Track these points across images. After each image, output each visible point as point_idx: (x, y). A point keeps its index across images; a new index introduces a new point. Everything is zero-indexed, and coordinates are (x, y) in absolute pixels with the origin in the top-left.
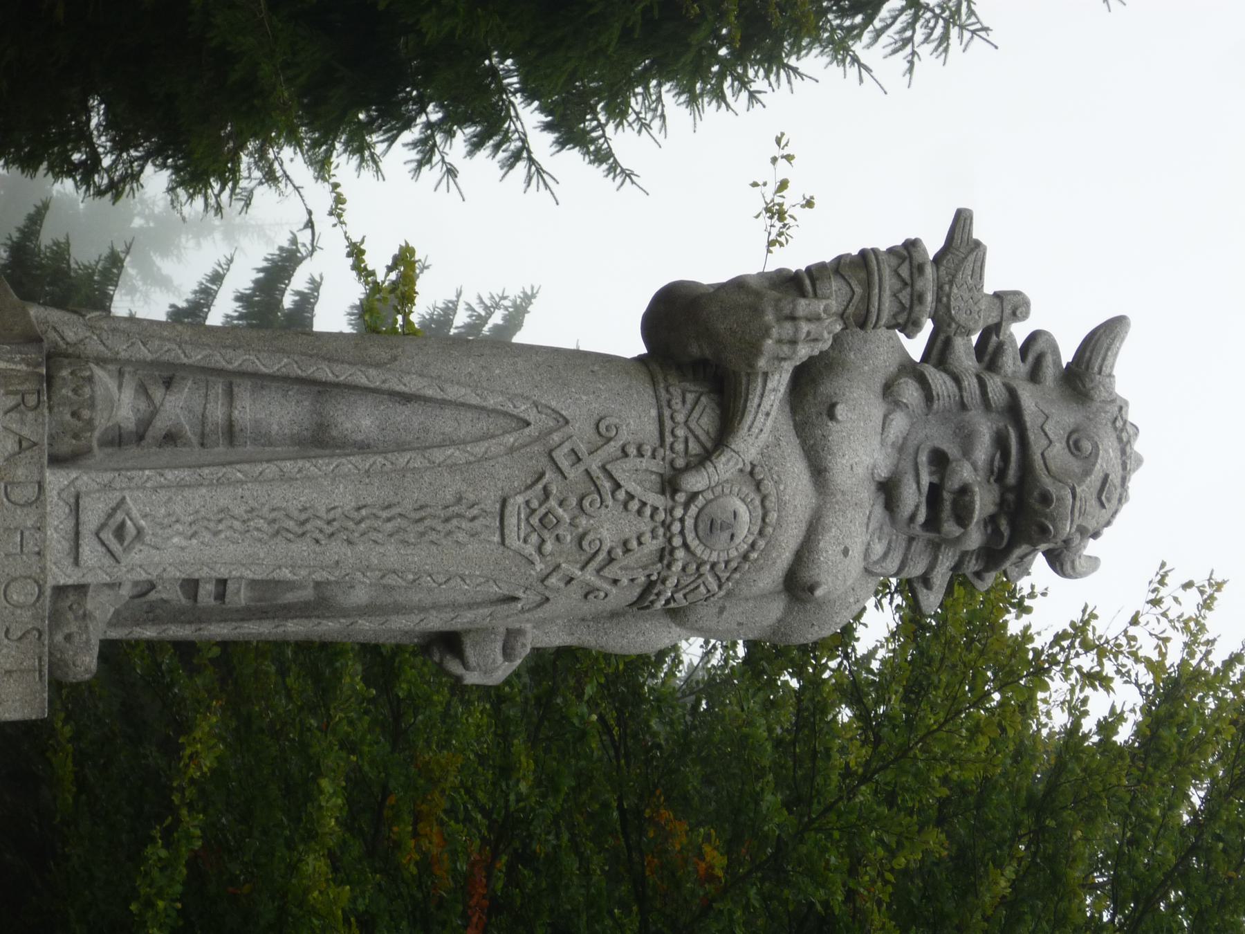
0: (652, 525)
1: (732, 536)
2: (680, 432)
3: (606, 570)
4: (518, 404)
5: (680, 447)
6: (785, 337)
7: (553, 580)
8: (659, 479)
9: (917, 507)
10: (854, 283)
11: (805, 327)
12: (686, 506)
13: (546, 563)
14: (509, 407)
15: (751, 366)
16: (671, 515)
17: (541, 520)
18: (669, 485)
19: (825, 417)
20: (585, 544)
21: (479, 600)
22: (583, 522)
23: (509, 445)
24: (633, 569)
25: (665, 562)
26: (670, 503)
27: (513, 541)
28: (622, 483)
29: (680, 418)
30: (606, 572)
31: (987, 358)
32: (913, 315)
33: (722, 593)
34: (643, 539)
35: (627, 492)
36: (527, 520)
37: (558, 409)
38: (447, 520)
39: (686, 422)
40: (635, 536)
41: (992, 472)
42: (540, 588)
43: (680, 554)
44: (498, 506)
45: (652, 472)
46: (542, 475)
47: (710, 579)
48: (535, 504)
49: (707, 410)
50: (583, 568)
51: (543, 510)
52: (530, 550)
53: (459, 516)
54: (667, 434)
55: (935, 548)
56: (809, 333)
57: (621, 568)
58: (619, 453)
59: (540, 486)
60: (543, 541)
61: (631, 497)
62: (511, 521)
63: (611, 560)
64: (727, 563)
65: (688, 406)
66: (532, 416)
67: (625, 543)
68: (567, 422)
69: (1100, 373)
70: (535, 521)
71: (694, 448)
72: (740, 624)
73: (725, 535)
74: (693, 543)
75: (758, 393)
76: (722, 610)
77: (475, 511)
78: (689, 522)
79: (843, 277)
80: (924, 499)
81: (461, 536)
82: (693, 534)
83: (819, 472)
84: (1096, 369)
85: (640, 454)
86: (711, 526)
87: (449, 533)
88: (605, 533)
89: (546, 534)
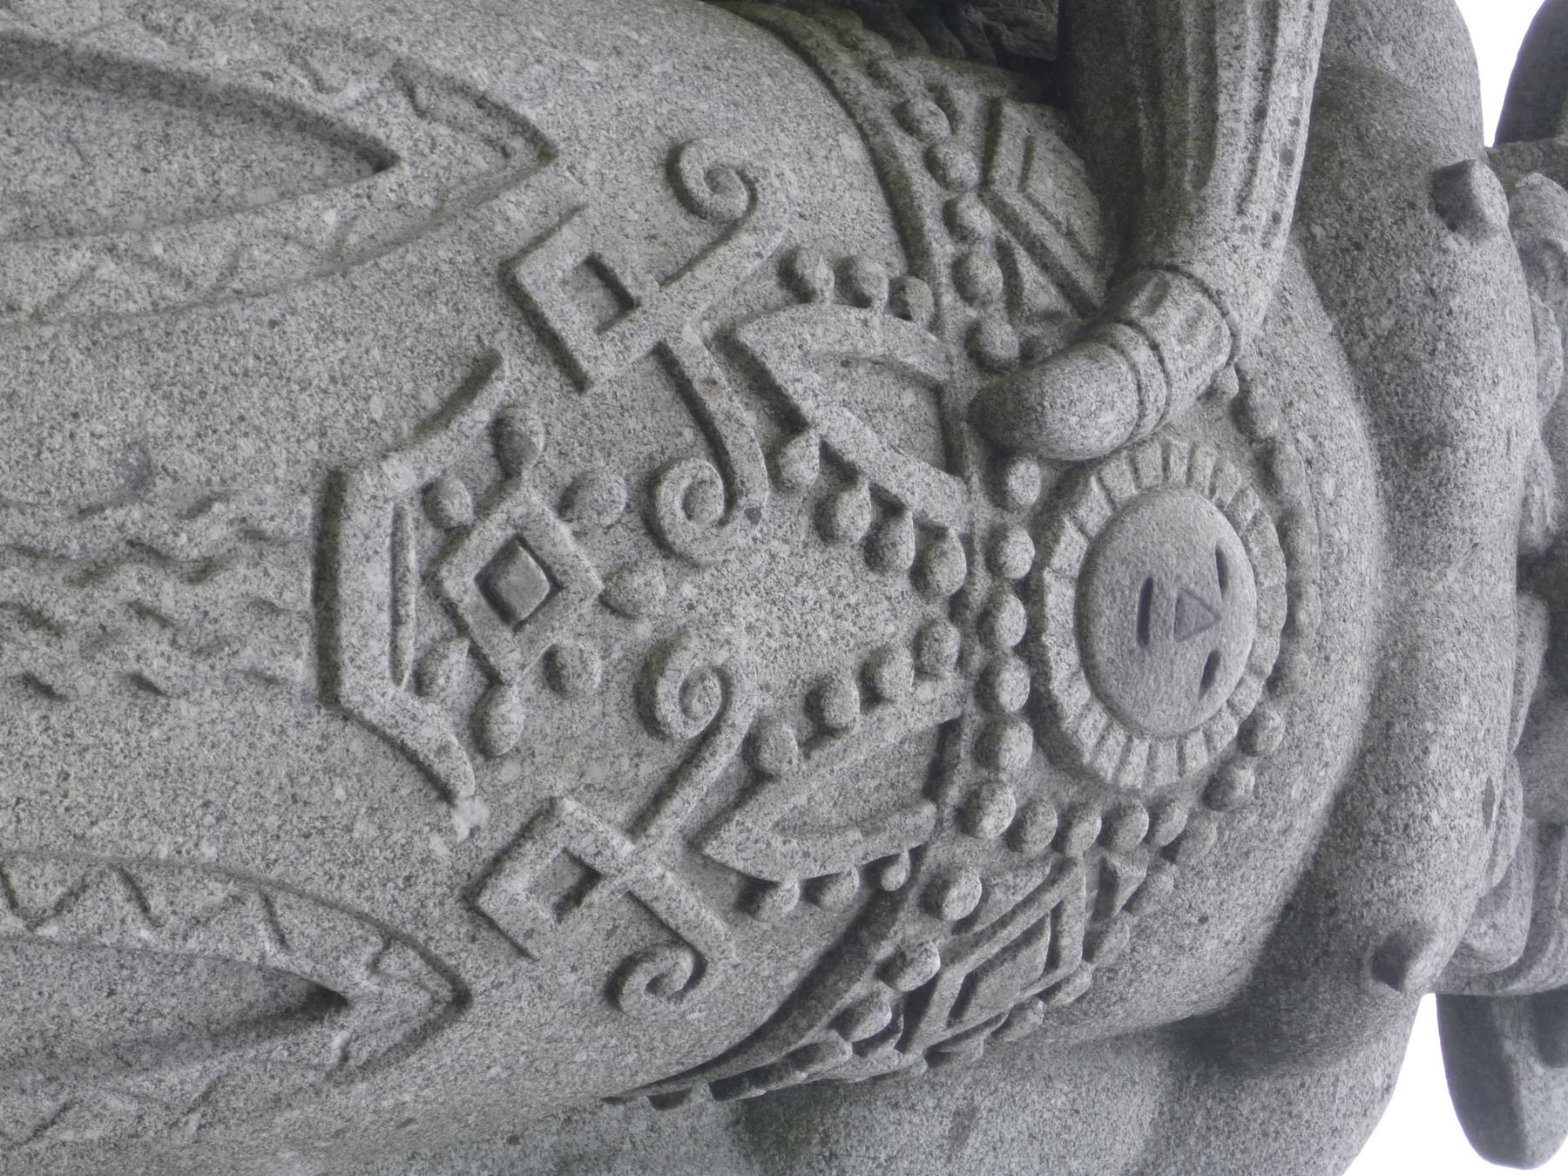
0: (913, 611)
1: (1212, 663)
2: (979, 218)
3: (731, 832)
5: (989, 275)
7: (518, 893)
8: (927, 411)
12: (1044, 526)
13: (492, 795)
14: (303, 93)
16: (994, 566)
17: (486, 583)
18: (984, 426)
19: (1429, 216)
20: (667, 690)
21: (159, 1026)
22: (652, 580)
23: (323, 240)
25: (954, 794)
26: (985, 514)
27: (372, 686)
28: (807, 407)
29: (964, 166)
30: (729, 848)
33: (1084, 981)
34: (887, 673)
35: (829, 456)
36: (431, 580)
37: (502, 91)
38: (93, 574)
39: (985, 183)
40: (852, 661)
43: (1019, 747)
44: (306, 507)
45: (907, 376)
46: (481, 371)
48: (459, 506)
49: (1040, 149)
50: (637, 826)
51: (492, 534)
52: (435, 727)
53: (150, 553)
54: (933, 226)
57: (781, 827)
58: (770, 286)
59: (480, 415)
60: (493, 681)
61: (840, 471)
62: (366, 581)
63: (755, 777)
64: (1157, 810)
65: (969, 133)
66: (392, 124)
67: (814, 701)
68: (545, 152)
70: (460, 583)
73: (1192, 659)
74: (1072, 696)
75: (1251, 64)
76: (964, 1122)
77: (213, 532)
78: (1059, 599)
81: (154, 655)
82: (1072, 656)
83: (1413, 449)
85: (852, 293)
87: (102, 639)
88: (743, 652)
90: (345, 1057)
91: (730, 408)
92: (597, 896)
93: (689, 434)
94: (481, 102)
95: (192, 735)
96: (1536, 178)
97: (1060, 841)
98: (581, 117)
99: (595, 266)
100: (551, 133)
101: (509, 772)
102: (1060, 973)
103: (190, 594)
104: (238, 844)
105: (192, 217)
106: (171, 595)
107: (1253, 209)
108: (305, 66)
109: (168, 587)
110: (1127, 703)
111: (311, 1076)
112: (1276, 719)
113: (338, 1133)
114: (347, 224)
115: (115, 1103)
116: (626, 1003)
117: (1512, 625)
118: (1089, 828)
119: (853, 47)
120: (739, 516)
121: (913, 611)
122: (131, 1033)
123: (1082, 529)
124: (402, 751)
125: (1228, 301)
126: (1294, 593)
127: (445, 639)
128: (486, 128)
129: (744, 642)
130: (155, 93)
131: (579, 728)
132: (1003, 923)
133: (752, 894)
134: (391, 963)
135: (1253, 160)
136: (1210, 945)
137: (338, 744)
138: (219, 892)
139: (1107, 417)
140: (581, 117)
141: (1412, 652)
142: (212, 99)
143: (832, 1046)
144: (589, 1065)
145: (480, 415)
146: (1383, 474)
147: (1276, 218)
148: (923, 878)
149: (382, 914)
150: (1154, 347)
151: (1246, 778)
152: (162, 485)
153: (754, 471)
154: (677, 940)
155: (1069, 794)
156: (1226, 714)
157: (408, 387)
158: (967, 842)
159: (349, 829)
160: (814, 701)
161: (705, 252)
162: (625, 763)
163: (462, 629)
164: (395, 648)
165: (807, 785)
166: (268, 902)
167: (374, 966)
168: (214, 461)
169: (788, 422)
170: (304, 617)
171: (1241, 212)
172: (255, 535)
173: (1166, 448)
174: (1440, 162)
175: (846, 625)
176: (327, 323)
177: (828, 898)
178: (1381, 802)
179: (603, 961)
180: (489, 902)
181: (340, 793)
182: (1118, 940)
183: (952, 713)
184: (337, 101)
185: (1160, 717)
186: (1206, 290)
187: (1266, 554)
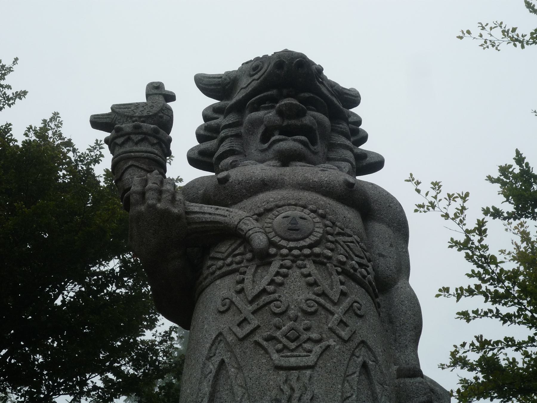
0: (295, 269)
1: (301, 218)
2: (229, 260)
3: (333, 298)
4: (209, 370)
5: (238, 258)
6: (156, 195)
7: (344, 334)
8: (261, 268)
9: (295, 140)
10: (126, 166)
11: (150, 184)
12: (280, 247)
13: (328, 338)
14: (212, 375)
15: (178, 217)
16: (287, 255)
17: (292, 341)
18: (263, 258)
20: (309, 310)
21: (370, 393)
22: (291, 313)
23: (236, 371)
24: (332, 282)
25: (325, 261)
26: (278, 257)
27: (311, 359)
28: (261, 288)
29: (220, 263)
30: (336, 298)
31: (215, 135)
32: (149, 132)
34: (305, 273)
35: (269, 284)
36: (293, 350)
37: (211, 342)
39: (223, 259)
40: (303, 279)
41: (273, 107)
42: (352, 344)
43: (317, 250)
45: (256, 272)
46: (257, 343)
47: (340, 238)
48: (280, 346)
49: (217, 250)
50: (332, 314)
51: (284, 340)
52: (317, 349)
55: (332, 146)
56: (154, 183)
59: (265, 343)
60: (309, 339)
61: (272, 282)
62: (293, 361)
63: (323, 294)
64: (326, 226)
66: (216, 360)
67: (310, 285)
68: (220, 334)
69: (221, 77)
70: (293, 345)
71: (241, 250)
72: (391, 245)
73: (301, 222)
74: (308, 241)
77: (286, 388)
78: (292, 244)
79: (123, 173)
80: (290, 138)
82: (301, 242)
84: (220, 80)
86: (294, 229)
89: (305, 336)
90: (373, 361)
91: (261, 302)
92: (345, 320)
93: (267, 308)
94: (212, 345)
95: (320, 390)
96: (220, 166)
97: (332, 242)
98: (214, 328)
99: (239, 325)
100: (217, 333)
101: (324, 336)
102: (355, 241)
103: (296, 391)
104: (338, 381)
105: (233, 393)
106: (297, 395)
107: (226, 214)
108: (207, 375)
109: (295, 395)
110: (309, 232)
111: (377, 367)
112: (311, 207)
113: (387, 362)
114: (233, 367)
115: (383, 400)
116: (363, 314)
117: (294, 167)
118: (329, 237)
119: (201, 282)
120: (280, 299)
121: (295, 269)
122: (371, 398)
123: (280, 241)
124: (321, 354)
125: (241, 218)
126: (289, 205)
127: (302, 348)
128: (217, 344)
129: (301, 297)
130: (213, 400)
131: (316, 324)
132: (346, 251)
133: (343, 294)
134: (357, 354)
135: (218, 215)
136: (348, 215)
137: (321, 365)
138: (346, 384)
139: (261, 238)
140: (214, 328)
141: (299, 184)
142: (213, 390)
143: (369, 279)
144: (373, 320)
145: (265, 343)
146: (269, 190)
147: (227, 210)
148: (339, 265)
149: (349, 356)
150: (249, 230)
151: (320, 211)
152: (278, 397)
153: (272, 296)
154: (352, 306)
155: (324, 241)
156: (310, 215)
157: (260, 356)
158: (333, 258)
159: (335, 363)
160: (310, 285)
161: (236, 306)
162: (322, 316)
163: (301, 345)
164: (304, 356)
165: (325, 285)
166: (348, 376)
167: (358, 357)
168: (274, 388)
169: (264, 291)
170: (300, 372)
171: (226, 216)
172: (286, 381)
173: (266, 227)
174: (217, 183)
175: (297, 280)
176: (250, 370)
177: (344, 281)
178: (324, 188)
179: (355, 318)
180: (346, 338)
181: (329, 364)
182: (348, 231)
183: (311, 261)
184: (213, 369)
185: (311, 226)
186: (240, 222)
187: (283, 210)
